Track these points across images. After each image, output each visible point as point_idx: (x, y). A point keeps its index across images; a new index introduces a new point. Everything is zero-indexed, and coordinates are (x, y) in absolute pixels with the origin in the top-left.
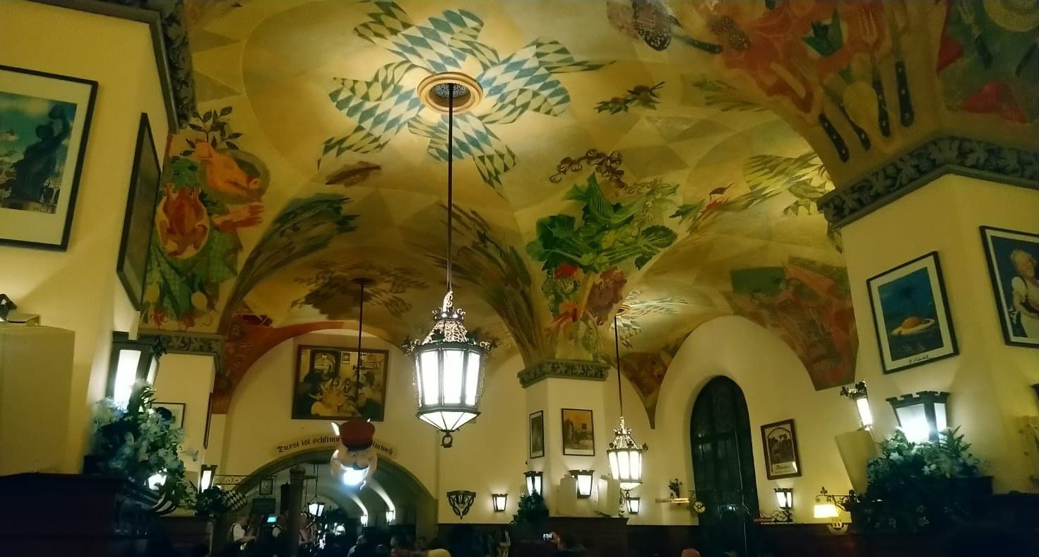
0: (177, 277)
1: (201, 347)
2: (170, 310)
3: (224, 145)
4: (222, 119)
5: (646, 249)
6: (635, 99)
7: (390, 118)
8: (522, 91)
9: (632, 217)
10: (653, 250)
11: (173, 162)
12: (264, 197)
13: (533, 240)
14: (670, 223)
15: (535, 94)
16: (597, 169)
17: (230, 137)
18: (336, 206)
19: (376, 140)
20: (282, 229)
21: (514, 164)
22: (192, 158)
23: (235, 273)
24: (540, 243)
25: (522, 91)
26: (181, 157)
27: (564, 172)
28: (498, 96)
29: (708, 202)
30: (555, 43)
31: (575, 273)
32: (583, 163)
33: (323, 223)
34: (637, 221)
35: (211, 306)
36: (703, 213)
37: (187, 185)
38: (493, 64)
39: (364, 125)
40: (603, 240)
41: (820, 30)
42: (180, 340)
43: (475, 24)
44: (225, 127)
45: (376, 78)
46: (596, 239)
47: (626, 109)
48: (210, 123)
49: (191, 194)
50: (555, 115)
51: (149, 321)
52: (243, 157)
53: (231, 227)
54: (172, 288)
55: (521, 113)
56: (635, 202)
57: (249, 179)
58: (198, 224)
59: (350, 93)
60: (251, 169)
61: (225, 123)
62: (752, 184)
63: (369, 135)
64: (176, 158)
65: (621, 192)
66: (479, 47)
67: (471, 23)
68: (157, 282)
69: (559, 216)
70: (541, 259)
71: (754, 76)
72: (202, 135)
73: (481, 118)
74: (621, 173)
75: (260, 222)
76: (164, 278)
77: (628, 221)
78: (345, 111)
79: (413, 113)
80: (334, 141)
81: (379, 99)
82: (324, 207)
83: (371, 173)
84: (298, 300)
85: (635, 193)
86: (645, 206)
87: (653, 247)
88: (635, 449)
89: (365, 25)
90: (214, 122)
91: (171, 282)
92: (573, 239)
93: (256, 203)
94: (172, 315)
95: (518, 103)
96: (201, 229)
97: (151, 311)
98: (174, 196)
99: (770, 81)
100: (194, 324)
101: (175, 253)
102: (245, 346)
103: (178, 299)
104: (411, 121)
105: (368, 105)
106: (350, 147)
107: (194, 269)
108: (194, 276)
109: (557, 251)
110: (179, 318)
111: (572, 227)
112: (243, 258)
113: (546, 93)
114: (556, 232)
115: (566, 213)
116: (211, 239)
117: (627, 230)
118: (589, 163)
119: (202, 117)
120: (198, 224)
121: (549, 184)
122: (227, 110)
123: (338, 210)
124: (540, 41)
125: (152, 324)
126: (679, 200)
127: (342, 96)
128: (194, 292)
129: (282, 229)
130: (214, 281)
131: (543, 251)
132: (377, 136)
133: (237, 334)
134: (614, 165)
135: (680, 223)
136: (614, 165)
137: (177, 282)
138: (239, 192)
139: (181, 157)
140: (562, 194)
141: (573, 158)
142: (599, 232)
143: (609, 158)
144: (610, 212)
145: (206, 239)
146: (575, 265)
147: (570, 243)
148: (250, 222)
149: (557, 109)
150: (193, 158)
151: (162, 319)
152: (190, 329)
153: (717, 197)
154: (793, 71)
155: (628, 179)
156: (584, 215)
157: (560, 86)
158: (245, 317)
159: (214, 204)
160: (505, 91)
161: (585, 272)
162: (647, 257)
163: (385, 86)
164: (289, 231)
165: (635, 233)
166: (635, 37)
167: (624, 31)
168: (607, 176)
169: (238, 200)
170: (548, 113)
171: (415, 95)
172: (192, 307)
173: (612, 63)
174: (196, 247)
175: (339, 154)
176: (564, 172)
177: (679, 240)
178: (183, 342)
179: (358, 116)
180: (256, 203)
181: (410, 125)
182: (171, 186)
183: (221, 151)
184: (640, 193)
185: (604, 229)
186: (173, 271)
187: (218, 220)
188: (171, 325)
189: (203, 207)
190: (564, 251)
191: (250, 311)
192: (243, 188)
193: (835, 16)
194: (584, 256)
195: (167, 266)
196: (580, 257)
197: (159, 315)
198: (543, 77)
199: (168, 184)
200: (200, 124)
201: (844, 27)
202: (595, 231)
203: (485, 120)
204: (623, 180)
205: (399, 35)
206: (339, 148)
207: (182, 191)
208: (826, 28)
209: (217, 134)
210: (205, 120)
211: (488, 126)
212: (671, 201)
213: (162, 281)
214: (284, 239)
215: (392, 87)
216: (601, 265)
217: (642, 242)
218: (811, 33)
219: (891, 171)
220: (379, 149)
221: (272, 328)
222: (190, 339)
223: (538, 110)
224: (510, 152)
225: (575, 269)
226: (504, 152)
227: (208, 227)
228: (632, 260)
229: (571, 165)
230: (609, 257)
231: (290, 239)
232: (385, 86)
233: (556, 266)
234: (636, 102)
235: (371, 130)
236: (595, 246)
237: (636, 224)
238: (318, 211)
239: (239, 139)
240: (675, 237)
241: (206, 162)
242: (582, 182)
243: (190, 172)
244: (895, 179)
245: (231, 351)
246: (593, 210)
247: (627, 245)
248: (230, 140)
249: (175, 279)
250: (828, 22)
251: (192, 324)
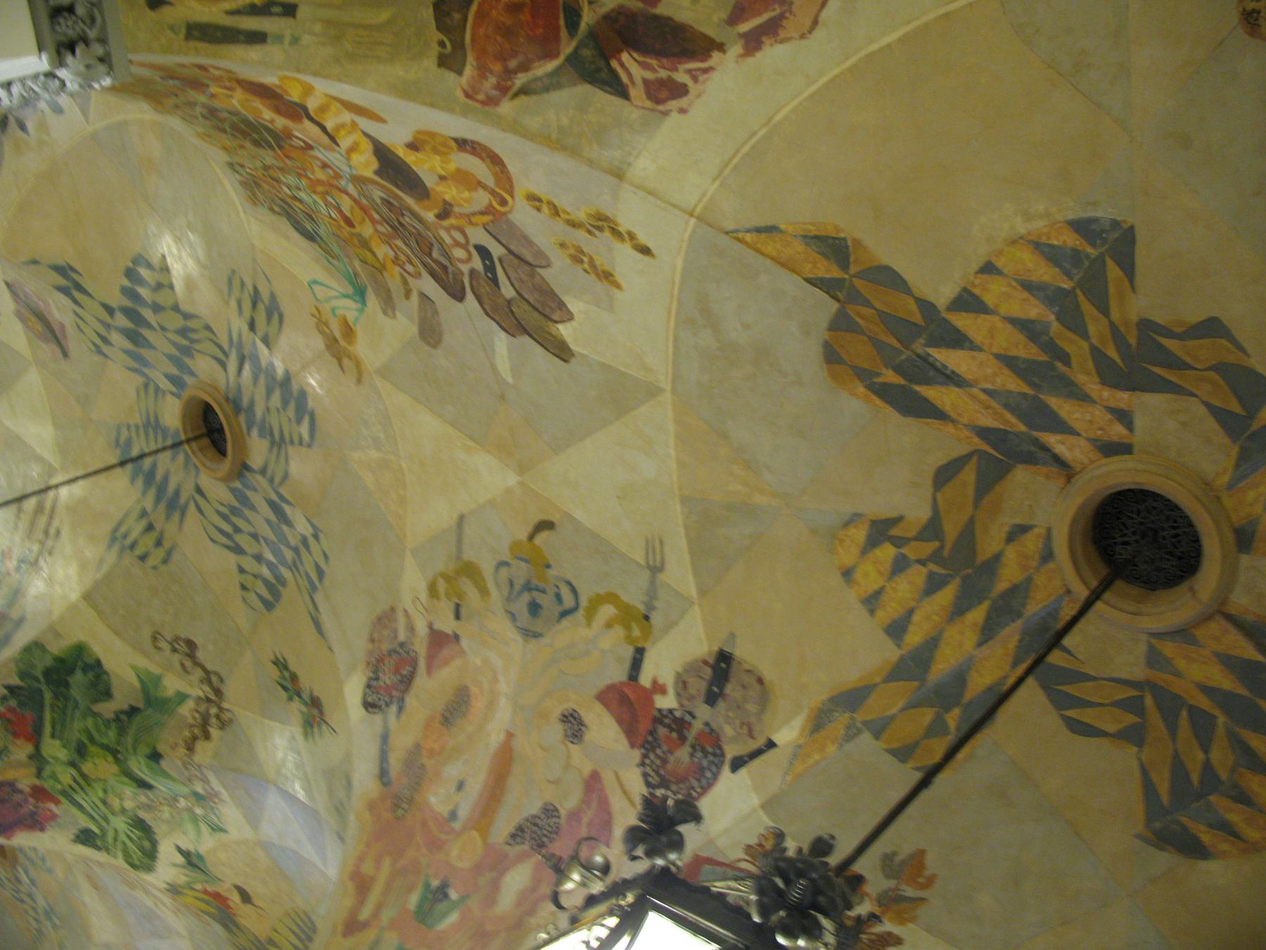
5: (110, 835)
6: (306, 704)
7: (145, 352)
8: (255, 536)
9: (149, 787)
10: (115, 847)
13: (48, 647)
14: (167, 850)
15: (259, 558)
16: (200, 698)
19: (105, 340)
21: (155, 568)
24: (48, 662)
25: (255, 536)
27: (174, 650)
28: (237, 504)
29: (222, 889)
30: (326, 557)
31: (20, 742)
32: (199, 673)
34: (148, 797)
36: (205, 892)
38: (271, 481)
40: (97, 761)
41: (441, 893)
43: (306, 436)
45: (187, 316)
46: (93, 749)
47: (290, 699)
50: (244, 599)
55: (228, 547)
56: (173, 779)
59: (153, 284)
62: (276, 937)
65: (182, 751)
66: (283, 452)
67: (304, 430)
69: (106, 673)
70: (23, 675)
71: (368, 845)
73: (199, 490)
74: (207, 736)
77: (143, 785)
78: (126, 283)
79: (165, 385)
80: (75, 276)
81: (163, 329)
83: (54, 347)
85: (186, 773)
86: (175, 800)
87: (119, 846)
89: (243, 284)
92: (78, 713)
95: (239, 538)
99: (368, 868)
104: (152, 387)
109: (48, 696)
111: (96, 701)
113: (265, 572)
114: (78, 679)
115: (115, 682)
117: (129, 791)
118: (202, 681)
121: (147, 632)
124: (321, 536)
126: (206, 844)
127: (144, 272)
131: (38, 673)
134: (213, 720)
135: (175, 865)
136: (213, 720)
140: (142, 662)
141: (200, 654)
142: (105, 747)
143: (220, 708)
144: (144, 750)
146: (35, 737)
147: (69, 712)
149: (252, 598)
153: (235, 898)
154: (388, 887)
155: (204, 751)
156: (122, 712)
157: (280, 588)
160: (247, 512)
161: (30, 757)
162: (99, 843)
163: (183, 332)
165: (129, 804)
166: (368, 664)
167: (370, 646)
168: (195, 719)
170: (244, 588)
171: (189, 380)
173: (331, 649)
176: (174, 650)
177: (148, 877)
179: (127, 303)
181: (146, 386)
184: (190, 780)
185: (115, 753)
190: (52, 706)
193: (463, 898)
194: (57, 743)
196: (53, 736)
198: (283, 562)
201: (454, 917)
202: (105, 741)
203: (197, 497)
204: (200, 745)
205: (252, 335)
206: (69, 288)
208: (446, 895)
211: (192, 507)
212: (199, 832)
215: (185, 342)
216: (54, 777)
217: (120, 823)
218: (435, 883)
223: (242, 570)
224: (169, 554)
225: (28, 738)
226: (167, 544)
228: (84, 822)
229: (187, 655)
230: (72, 783)
232: (183, 332)
233: (21, 704)
234: (304, 709)
235: (117, 329)
236: (81, 751)
237: (143, 799)
240: (149, 869)
242: (172, 684)
246: (138, 719)
247: (105, 803)
250: (453, 895)
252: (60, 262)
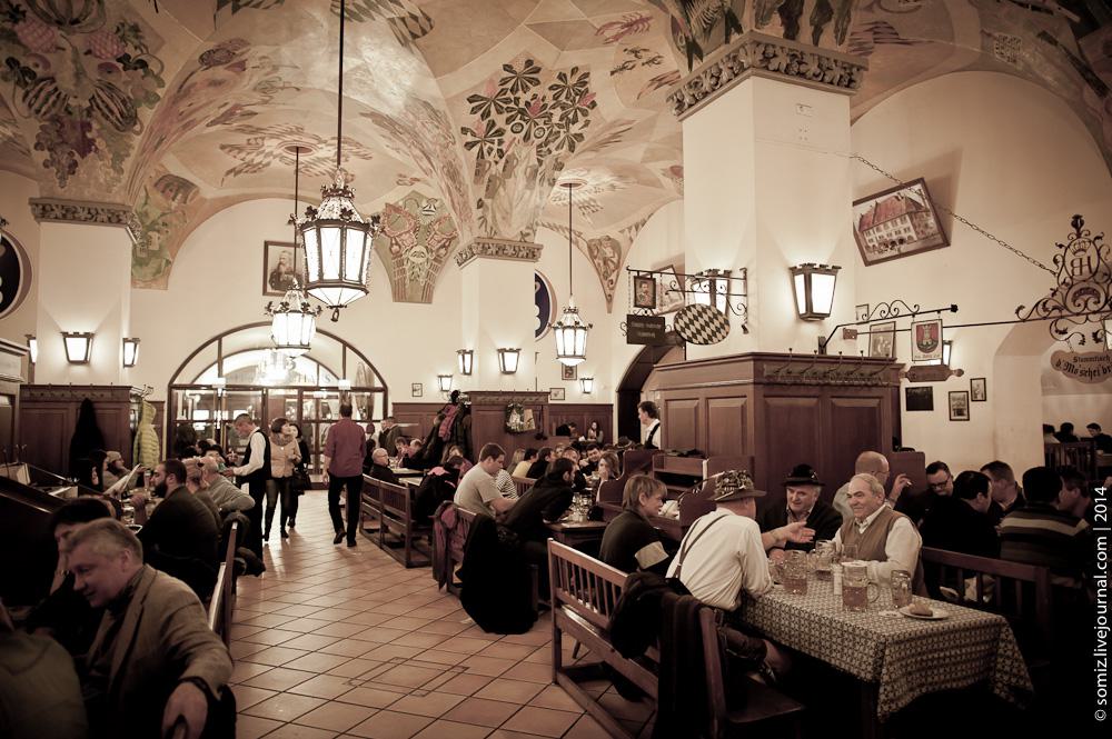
1: (109, 218)
42: (86, 211)
88: (582, 327)
178: (89, 213)
219: (714, 71)
222: (96, 209)
244: (718, 78)
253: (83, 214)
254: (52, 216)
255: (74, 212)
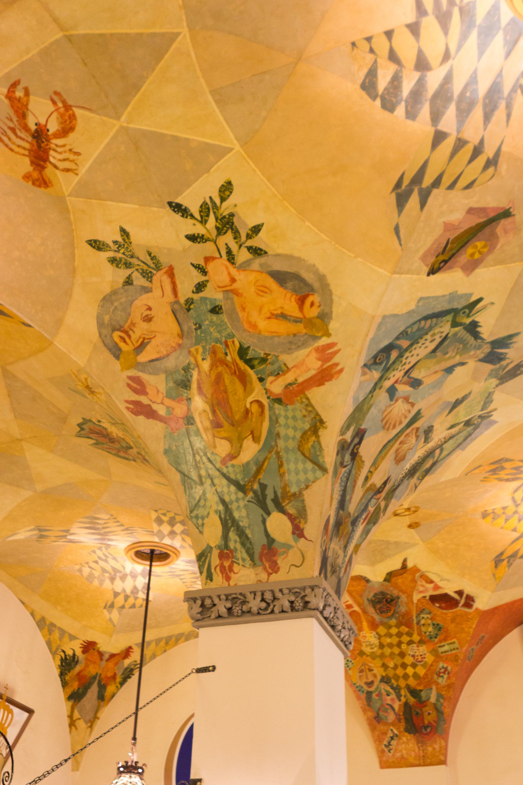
0: (241, 495)
2: (241, 553)
3: (243, 255)
4: (226, 208)
11: (189, 310)
12: (333, 326)
17: (249, 237)
18: (468, 321)
20: (387, 384)
22: (209, 293)
23: (324, 470)
26: (196, 297)
33: (463, 364)
35: (298, 532)
37: (217, 341)
39: (442, 126)
42: (259, 598)
44: (235, 220)
48: (212, 222)
49: (226, 354)
51: (215, 577)
52: (278, 266)
53: (296, 392)
54: (236, 515)
57: (301, 301)
58: (250, 399)
60: (298, 283)
61: (232, 215)
63: (460, 143)
64: (190, 302)
68: (216, 512)
72: (208, 248)
75: (341, 370)
76: (223, 502)
78: (401, 110)
80: (406, 182)
81: (447, 56)
82: (445, 327)
84: (502, 554)
90: (217, 219)
91: (234, 506)
93: (324, 341)
94: (244, 560)
96: (255, 408)
97: (215, 560)
98: (206, 365)
100: (279, 568)
101: (232, 457)
102: (446, 648)
103: (248, 532)
105: (434, 80)
106: (437, 183)
107: (261, 476)
108: (264, 487)
110: (254, 565)
112: (330, 440)
116: (274, 421)
119: (197, 215)
120: (250, 399)
122: (226, 189)
123: (473, 329)
125: (218, 579)
128: (269, 514)
129: (387, 384)
130: (294, 489)
132: (476, 142)
133: (430, 629)
137: (242, 503)
138: (293, 328)
139: (196, 297)
145: (266, 425)
148: (324, 376)
150: (213, 293)
151: (231, 569)
152: (274, 577)
158: (434, 599)
159: (264, 360)
164: (403, 389)
169: (294, 343)
172: (271, 541)
174: (256, 439)
175: (423, 203)
178: (263, 600)
180: (324, 341)
182: (197, 350)
183: (244, 267)
186: (233, 488)
187: (277, 386)
188: (246, 576)
189: (248, 369)
191: (437, 587)
192: (297, 321)
195: (225, 482)
197: (227, 564)
199: (193, 350)
200: (199, 229)
207: (214, 352)
209: (228, 238)
210: (203, 221)
213: (221, 508)
214: (400, 408)
215: (456, 12)
220: (491, 170)
221: (477, 609)
222: (272, 592)
227: (265, 402)
231: (413, 405)
235: (458, 132)
238: (438, 340)
239: (261, 234)
241: (231, 292)
243: (214, 317)
245: (429, 659)
248: (249, 243)
249: (237, 500)
251: (275, 568)
252: (393, 198)
253: (255, 604)
254: (213, 616)
255: (244, 602)
